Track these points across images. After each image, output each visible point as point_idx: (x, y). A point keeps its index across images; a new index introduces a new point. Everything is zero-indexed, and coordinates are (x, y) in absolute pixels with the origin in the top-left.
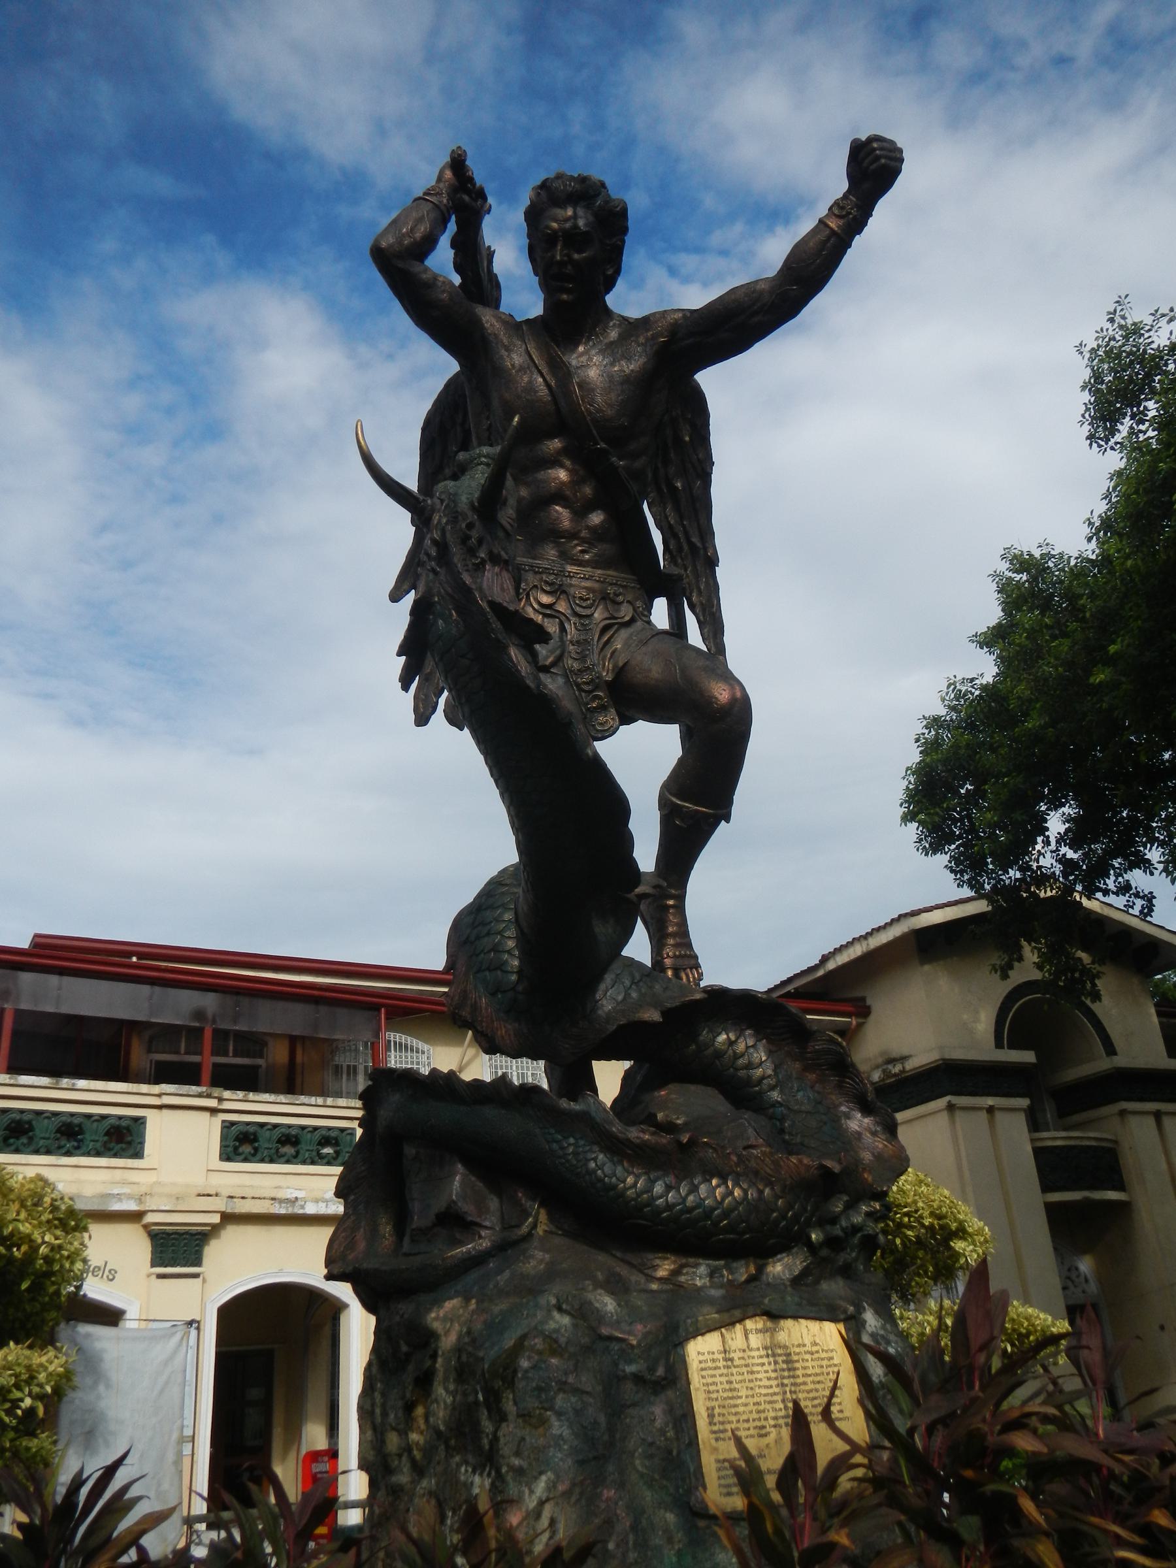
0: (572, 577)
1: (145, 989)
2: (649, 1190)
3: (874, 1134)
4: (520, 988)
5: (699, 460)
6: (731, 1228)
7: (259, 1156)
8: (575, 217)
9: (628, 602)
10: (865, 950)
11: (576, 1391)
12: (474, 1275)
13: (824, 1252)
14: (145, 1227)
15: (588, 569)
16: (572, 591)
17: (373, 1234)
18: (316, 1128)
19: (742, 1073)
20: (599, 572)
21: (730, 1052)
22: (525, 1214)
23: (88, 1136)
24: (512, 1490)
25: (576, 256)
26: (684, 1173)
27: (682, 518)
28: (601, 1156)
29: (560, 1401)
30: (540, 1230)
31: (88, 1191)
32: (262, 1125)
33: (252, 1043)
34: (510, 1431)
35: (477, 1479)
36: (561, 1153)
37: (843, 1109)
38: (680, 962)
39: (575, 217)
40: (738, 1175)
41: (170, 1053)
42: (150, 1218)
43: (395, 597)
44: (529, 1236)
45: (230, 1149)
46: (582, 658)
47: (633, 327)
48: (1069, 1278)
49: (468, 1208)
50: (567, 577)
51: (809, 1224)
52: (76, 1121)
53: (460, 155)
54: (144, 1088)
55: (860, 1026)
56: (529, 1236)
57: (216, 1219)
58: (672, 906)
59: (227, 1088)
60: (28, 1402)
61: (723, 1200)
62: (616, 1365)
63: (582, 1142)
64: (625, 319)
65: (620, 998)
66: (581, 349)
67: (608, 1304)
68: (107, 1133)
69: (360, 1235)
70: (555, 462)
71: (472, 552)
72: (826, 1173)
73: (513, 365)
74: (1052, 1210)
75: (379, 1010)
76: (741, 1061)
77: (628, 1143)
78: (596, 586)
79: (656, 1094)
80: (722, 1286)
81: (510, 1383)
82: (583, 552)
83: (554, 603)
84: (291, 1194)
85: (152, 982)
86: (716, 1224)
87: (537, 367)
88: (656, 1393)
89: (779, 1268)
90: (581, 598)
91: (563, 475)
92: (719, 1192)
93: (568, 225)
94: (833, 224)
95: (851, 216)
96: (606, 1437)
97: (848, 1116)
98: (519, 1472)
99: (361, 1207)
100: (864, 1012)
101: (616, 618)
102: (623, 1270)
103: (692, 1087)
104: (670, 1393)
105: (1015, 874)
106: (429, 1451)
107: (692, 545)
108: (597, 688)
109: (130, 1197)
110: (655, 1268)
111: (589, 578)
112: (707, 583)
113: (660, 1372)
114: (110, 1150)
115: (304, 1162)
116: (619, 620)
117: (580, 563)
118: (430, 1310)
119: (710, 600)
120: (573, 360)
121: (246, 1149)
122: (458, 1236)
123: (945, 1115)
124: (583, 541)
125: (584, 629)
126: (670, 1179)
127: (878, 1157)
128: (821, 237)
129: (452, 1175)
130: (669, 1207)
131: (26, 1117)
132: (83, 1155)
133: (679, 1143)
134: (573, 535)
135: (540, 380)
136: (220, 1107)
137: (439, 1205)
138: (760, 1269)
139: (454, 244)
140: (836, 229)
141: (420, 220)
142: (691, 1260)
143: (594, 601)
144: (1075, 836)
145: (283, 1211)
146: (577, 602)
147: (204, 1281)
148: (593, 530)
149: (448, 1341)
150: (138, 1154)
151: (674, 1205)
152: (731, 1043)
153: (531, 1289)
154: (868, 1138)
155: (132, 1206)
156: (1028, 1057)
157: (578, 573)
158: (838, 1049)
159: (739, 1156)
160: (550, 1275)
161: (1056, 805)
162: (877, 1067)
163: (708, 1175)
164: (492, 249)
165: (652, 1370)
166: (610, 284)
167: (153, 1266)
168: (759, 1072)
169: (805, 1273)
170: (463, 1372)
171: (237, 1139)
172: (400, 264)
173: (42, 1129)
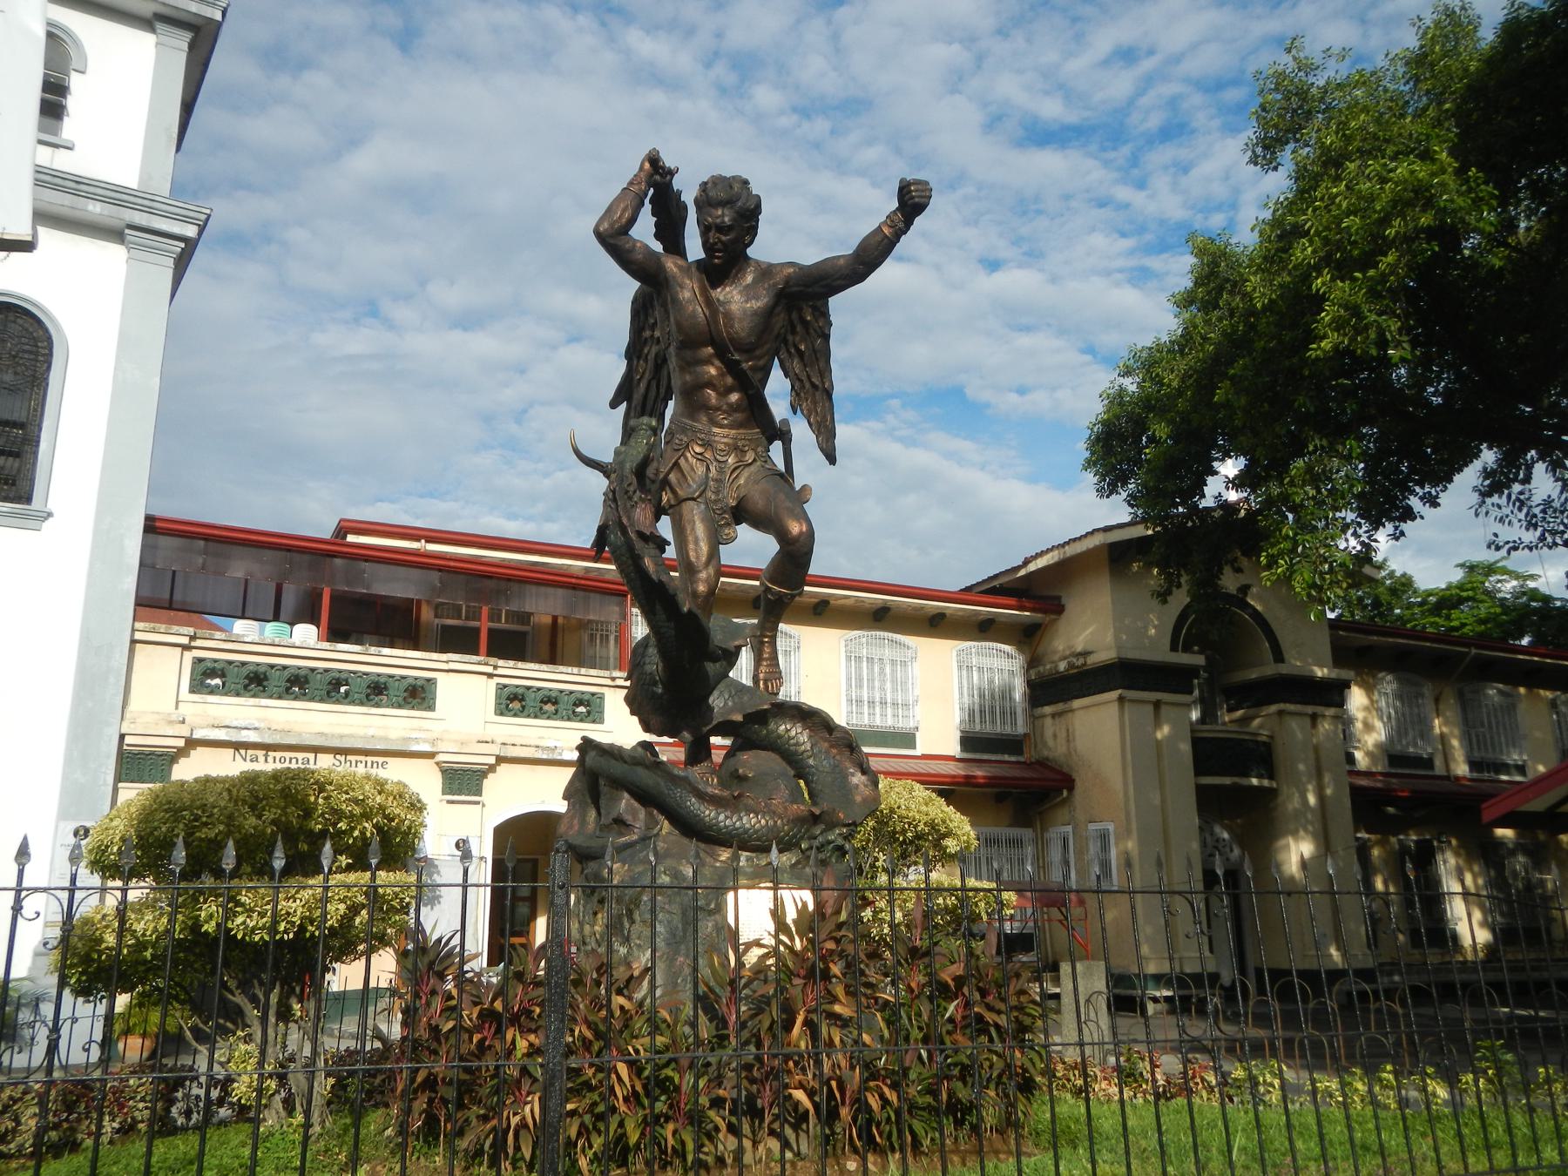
3: (866, 786)
6: (758, 839)
7: (526, 712)
8: (723, 215)
11: (669, 912)
12: (629, 851)
14: (437, 763)
17: (583, 822)
18: (571, 692)
25: (724, 238)
27: (805, 366)
30: (664, 832)
31: (394, 735)
32: (528, 688)
33: (524, 618)
39: (723, 215)
41: (453, 618)
42: (440, 758)
43: (614, 404)
44: (657, 835)
45: (503, 706)
46: (717, 492)
47: (766, 271)
48: (1210, 848)
49: (628, 818)
52: (382, 680)
54: (435, 656)
55: (1055, 620)
56: (657, 835)
57: (492, 760)
64: (757, 262)
66: (728, 289)
69: (576, 822)
70: (708, 362)
71: (630, 498)
72: (812, 814)
74: (1201, 791)
75: (626, 596)
77: (706, 794)
78: (730, 441)
81: (638, 907)
84: (551, 744)
91: (713, 371)
92: (753, 821)
93: (718, 221)
94: (886, 231)
97: (853, 775)
98: (639, 946)
100: (1057, 608)
103: (763, 753)
104: (717, 917)
107: (814, 386)
108: (725, 512)
109: (425, 741)
111: (727, 437)
112: (823, 406)
113: (712, 906)
115: (562, 719)
117: (721, 426)
119: (824, 417)
120: (719, 294)
121: (516, 705)
123: (1114, 708)
124: (724, 412)
125: (721, 471)
126: (728, 813)
127: (865, 800)
128: (879, 238)
129: (621, 800)
130: (726, 827)
134: (718, 409)
136: (496, 672)
137: (614, 815)
139: (651, 202)
141: (624, 210)
145: (545, 757)
147: (484, 805)
148: (730, 405)
150: (431, 708)
152: (788, 731)
155: (426, 748)
162: (1065, 658)
163: (749, 811)
165: (708, 905)
166: (751, 242)
167: (444, 793)
169: (798, 862)
171: (508, 699)
172: (612, 241)
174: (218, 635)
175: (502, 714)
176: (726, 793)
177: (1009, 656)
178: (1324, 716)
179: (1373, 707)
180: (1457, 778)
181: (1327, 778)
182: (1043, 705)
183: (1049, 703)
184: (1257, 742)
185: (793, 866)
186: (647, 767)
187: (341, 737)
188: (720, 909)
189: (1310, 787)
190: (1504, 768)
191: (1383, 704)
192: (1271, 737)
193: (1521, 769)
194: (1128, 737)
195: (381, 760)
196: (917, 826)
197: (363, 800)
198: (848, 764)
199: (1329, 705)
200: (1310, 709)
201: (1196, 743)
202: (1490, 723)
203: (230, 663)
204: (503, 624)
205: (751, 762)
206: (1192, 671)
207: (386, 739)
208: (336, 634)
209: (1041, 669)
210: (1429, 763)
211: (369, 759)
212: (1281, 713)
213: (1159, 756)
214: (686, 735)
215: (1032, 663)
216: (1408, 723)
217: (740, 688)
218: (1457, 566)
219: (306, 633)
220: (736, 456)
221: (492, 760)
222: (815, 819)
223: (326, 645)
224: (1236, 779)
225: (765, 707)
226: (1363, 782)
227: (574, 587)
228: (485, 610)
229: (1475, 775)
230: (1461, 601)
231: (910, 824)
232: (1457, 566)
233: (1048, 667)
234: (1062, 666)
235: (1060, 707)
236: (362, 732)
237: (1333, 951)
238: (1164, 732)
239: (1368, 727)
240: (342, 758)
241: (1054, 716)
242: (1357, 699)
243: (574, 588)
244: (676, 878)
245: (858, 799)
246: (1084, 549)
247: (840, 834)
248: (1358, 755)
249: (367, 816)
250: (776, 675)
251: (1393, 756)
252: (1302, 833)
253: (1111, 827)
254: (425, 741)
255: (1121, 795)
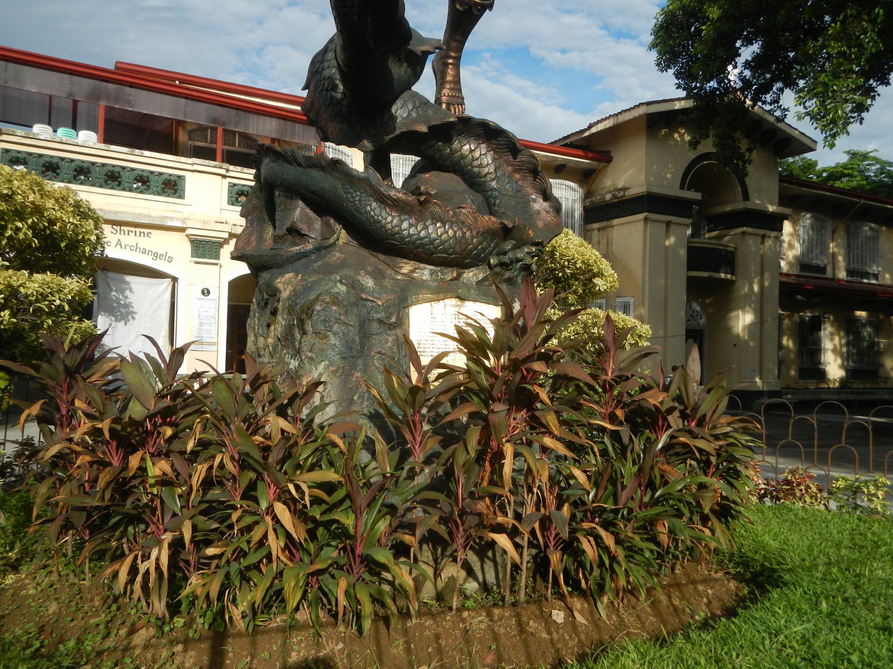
1: (183, 101)
2: (399, 226)
3: (547, 212)
4: (344, 103)
6: (445, 251)
12: (303, 261)
13: (498, 269)
17: (260, 239)
19: (476, 170)
21: (470, 156)
22: (334, 233)
23: (152, 184)
24: (307, 366)
26: (421, 218)
28: (374, 204)
29: (336, 327)
30: (341, 242)
34: (309, 339)
35: (292, 361)
36: (351, 200)
37: (533, 197)
38: (451, 100)
40: (452, 223)
42: (189, 231)
45: (234, 199)
48: (691, 316)
49: (303, 228)
51: (490, 253)
52: (145, 174)
54: (183, 159)
55: (605, 167)
56: (334, 243)
57: (226, 236)
58: (451, 64)
59: (231, 164)
60: (58, 302)
61: (441, 235)
62: (368, 313)
63: (364, 195)
65: (405, 115)
67: (369, 283)
68: (164, 183)
69: (253, 239)
74: (689, 279)
76: (475, 163)
77: (389, 197)
79: (423, 175)
80: (436, 281)
81: (310, 317)
85: (187, 97)
86: (436, 248)
88: (390, 329)
89: (472, 275)
92: (440, 231)
96: (359, 347)
97: (534, 201)
98: (311, 359)
99: (255, 223)
100: (607, 158)
102: (382, 266)
104: (398, 331)
105: (713, 84)
106: (275, 346)
109: (178, 219)
110: (401, 268)
113: (393, 320)
114: (164, 192)
118: (277, 278)
122: (297, 241)
123: (641, 224)
126: (413, 221)
127: (547, 225)
129: (296, 208)
130: (410, 236)
131: (116, 170)
132: (150, 194)
133: (419, 201)
136: (228, 174)
137: (288, 224)
138: (459, 275)
142: (422, 265)
144: (754, 64)
147: (221, 266)
149: (285, 294)
150: (181, 197)
151: (413, 235)
152: (471, 151)
153: (329, 270)
154: (543, 214)
155: (178, 224)
156: (698, 196)
158: (535, 161)
159: (454, 213)
160: (343, 265)
161: (748, 42)
163: (435, 219)
165: (389, 318)
168: (486, 170)
169: (485, 279)
170: (290, 310)
173: (125, 176)
174: (20, 131)
175: (233, 204)
176: (411, 198)
177: (573, 190)
178: (770, 237)
179: (795, 234)
180: (839, 280)
181: (766, 275)
182: (592, 223)
183: (596, 222)
184: (726, 251)
185: (479, 283)
186: (322, 169)
187: (116, 212)
188: (401, 323)
189: (756, 280)
190: (866, 275)
191: (801, 232)
192: (735, 249)
193: (876, 277)
194: (648, 244)
195: (146, 231)
196: (575, 263)
197: (10, 197)
198: (529, 190)
199: (773, 230)
200: (761, 232)
201: (690, 250)
202: (862, 248)
203: (30, 154)
204: (236, 148)
205: (434, 181)
206: (690, 202)
207: (149, 216)
208: (109, 138)
209: (594, 199)
210: (823, 270)
211: (138, 230)
212: (743, 233)
213: (667, 257)
214: (366, 143)
215: (587, 195)
216: (815, 245)
217: (425, 102)
218: (845, 152)
219: (87, 138)
221: (226, 236)
222: (506, 232)
223: (102, 146)
224: (712, 274)
225: (452, 120)
226: (785, 279)
227: (284, 118)
228: (220, 129)
229: (849, 278)
230: (844, 175)
231: (569, 261)
232: (845, 152)
233: (598, 197)
234: (608, 197)
235: (604, 223)
236: (131, 211)
237: (758, 380)
238: (671, 241)
239: (791, 246)
240: (118, 228)
241: (599, 230)
242: (787, 227)
243: (284, 119)
244: (354, 288)
245: (540, 224)
246: (632, 117)
247: (528, 253)
248: (783, 264)
249: (20, 214)
250: (458, 100)
251: (804, 265)
252: (748, 308)
253: (632, 300)
254: (178, 219)
255: (640, 281)
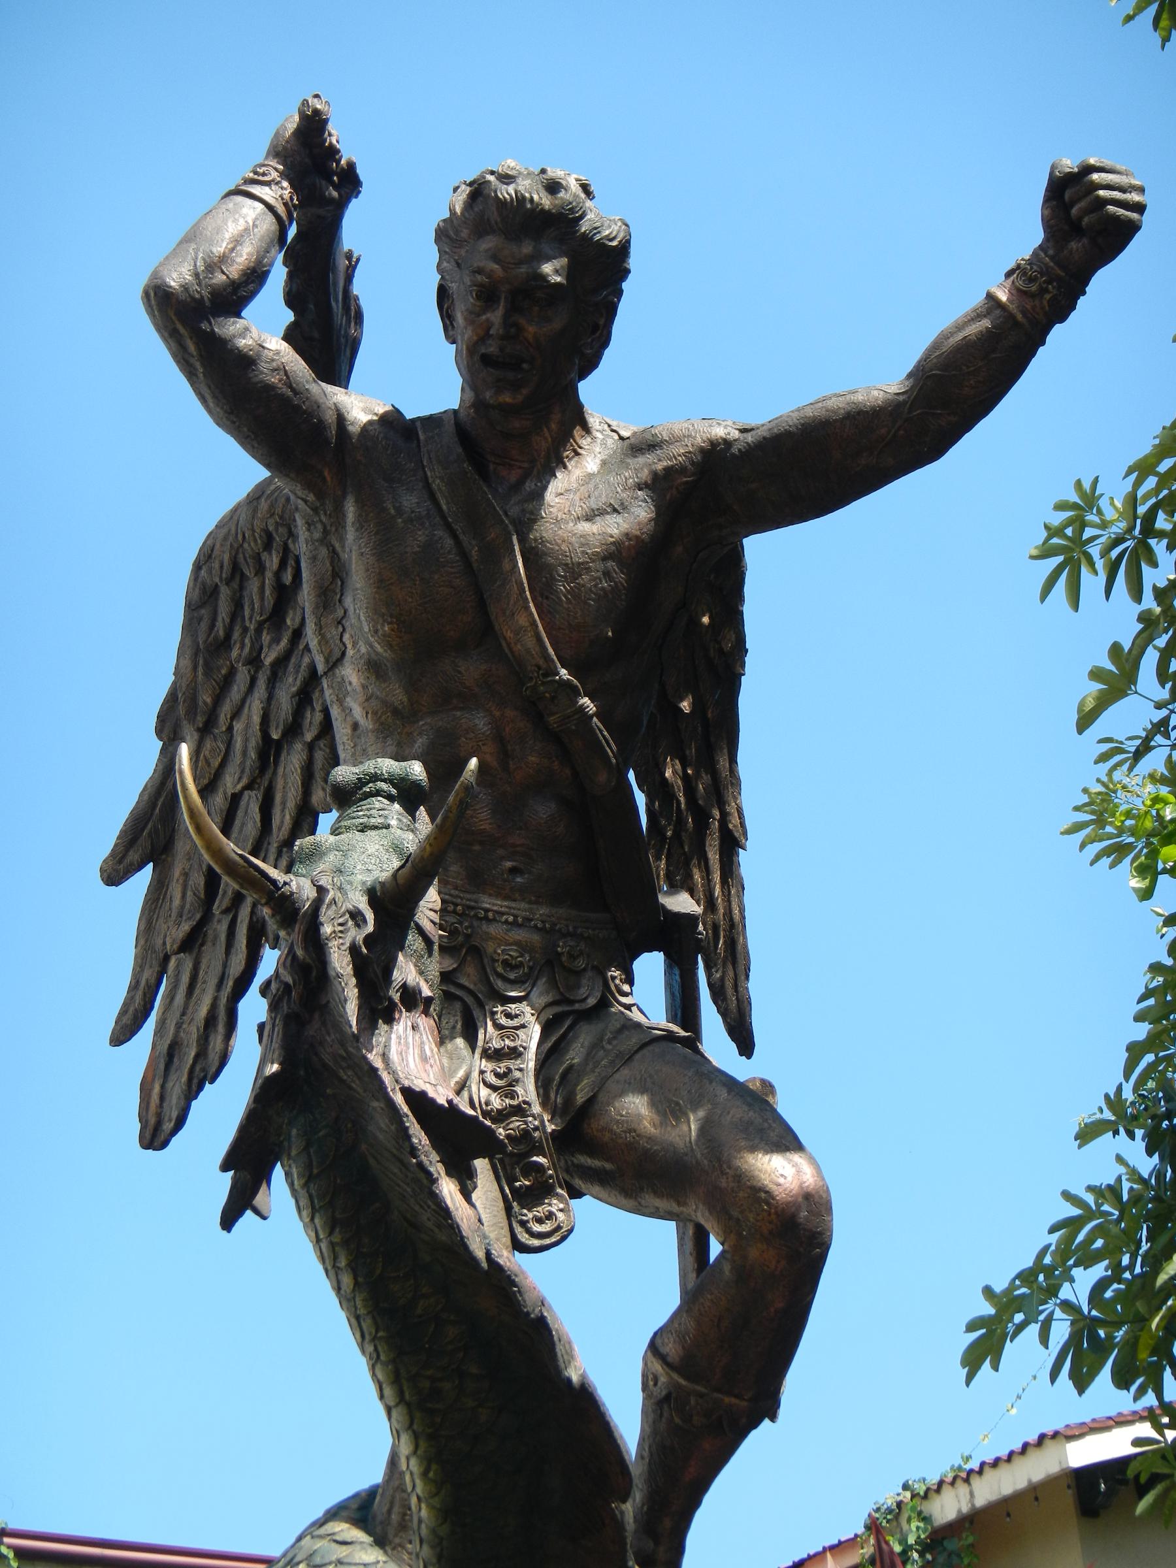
0: (494, 920)
5: (721, 651)
9: (594, 968)
10: (965, 1509)
15: (523, 905)
16: (490, 947)
20: (543, 910)
50: (481, 919)
53: (317, 112)
73: (399, 511)
82: (514, 871)
83: (454, 970)
87: (449, 527)
90: (506, 963)
95: (1048, 296)
101: (572, 1002)
116: (577, 1006)
135: (449, 542)
140: (1019, 317)
143: (530, 968)
146: (500, 970)
157: (503, 914)
164: (355, 255)
220: (553, 984)
246: (1022, 1484)
